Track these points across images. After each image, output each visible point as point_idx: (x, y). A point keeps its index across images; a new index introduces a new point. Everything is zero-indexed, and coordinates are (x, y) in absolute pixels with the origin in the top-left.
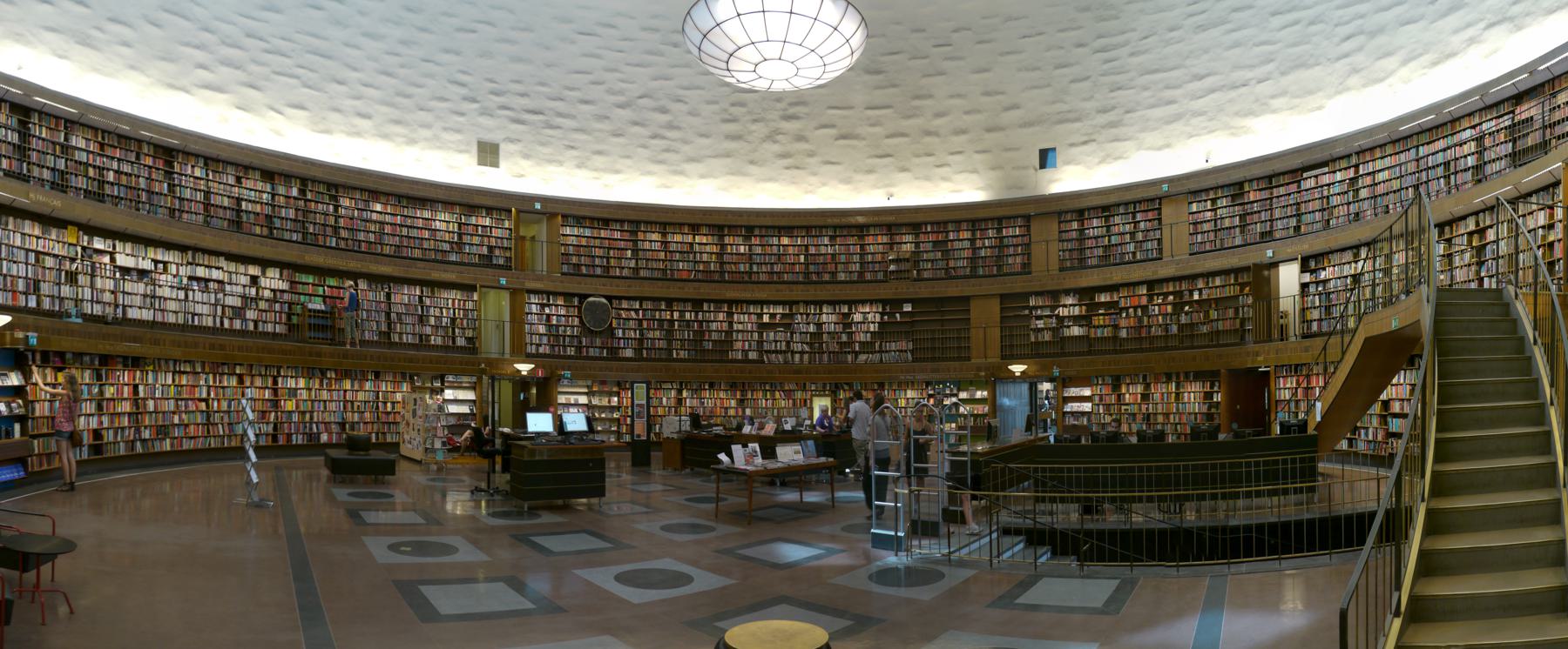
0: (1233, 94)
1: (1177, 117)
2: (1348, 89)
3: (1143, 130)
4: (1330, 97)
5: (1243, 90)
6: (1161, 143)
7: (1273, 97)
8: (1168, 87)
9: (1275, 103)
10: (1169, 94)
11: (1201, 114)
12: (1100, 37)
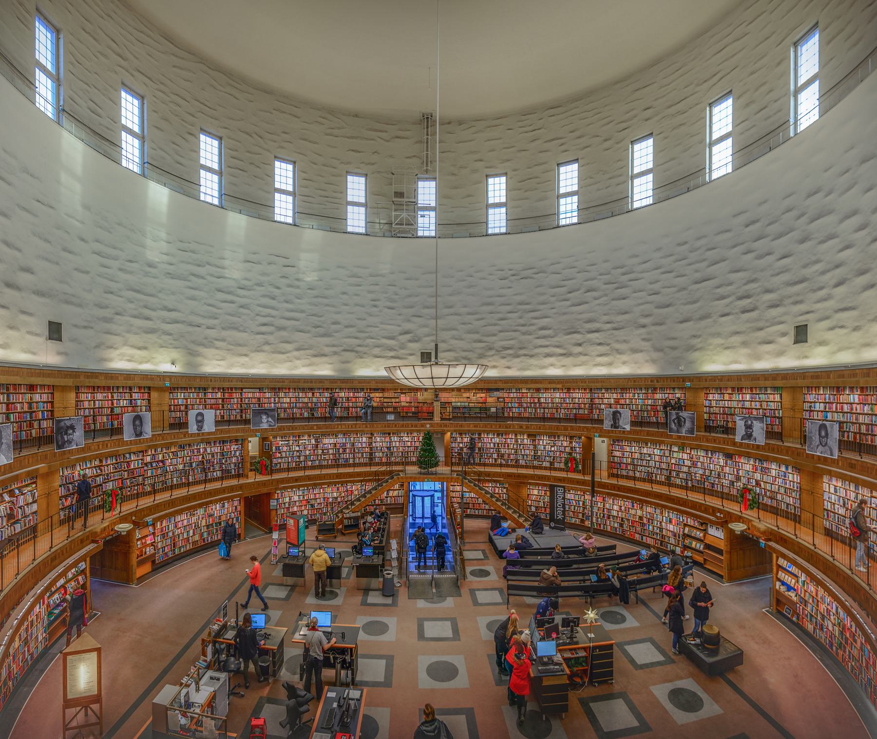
0: (191, 329)
1: (152, 331)
2: (263, 351)
3: (129, 332)
4: (252, 351)
5: (197, 329)
6: (141, 344)
7: (217, 340)
8: (146, 307)
9: (218, 344)
10: (147, 312)
11: (170, 334)
12: (97, 241)
